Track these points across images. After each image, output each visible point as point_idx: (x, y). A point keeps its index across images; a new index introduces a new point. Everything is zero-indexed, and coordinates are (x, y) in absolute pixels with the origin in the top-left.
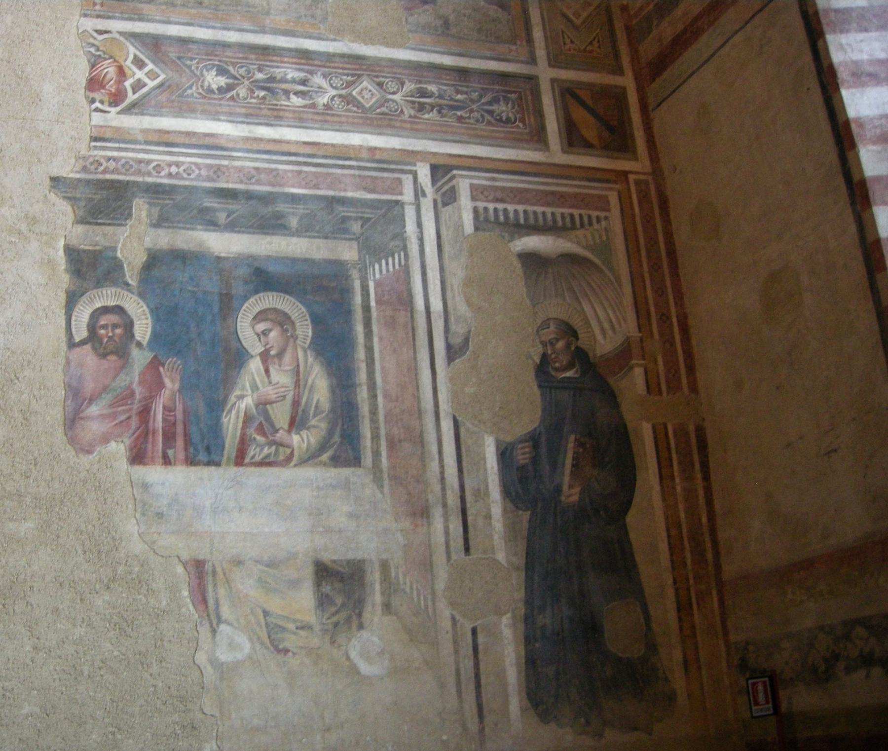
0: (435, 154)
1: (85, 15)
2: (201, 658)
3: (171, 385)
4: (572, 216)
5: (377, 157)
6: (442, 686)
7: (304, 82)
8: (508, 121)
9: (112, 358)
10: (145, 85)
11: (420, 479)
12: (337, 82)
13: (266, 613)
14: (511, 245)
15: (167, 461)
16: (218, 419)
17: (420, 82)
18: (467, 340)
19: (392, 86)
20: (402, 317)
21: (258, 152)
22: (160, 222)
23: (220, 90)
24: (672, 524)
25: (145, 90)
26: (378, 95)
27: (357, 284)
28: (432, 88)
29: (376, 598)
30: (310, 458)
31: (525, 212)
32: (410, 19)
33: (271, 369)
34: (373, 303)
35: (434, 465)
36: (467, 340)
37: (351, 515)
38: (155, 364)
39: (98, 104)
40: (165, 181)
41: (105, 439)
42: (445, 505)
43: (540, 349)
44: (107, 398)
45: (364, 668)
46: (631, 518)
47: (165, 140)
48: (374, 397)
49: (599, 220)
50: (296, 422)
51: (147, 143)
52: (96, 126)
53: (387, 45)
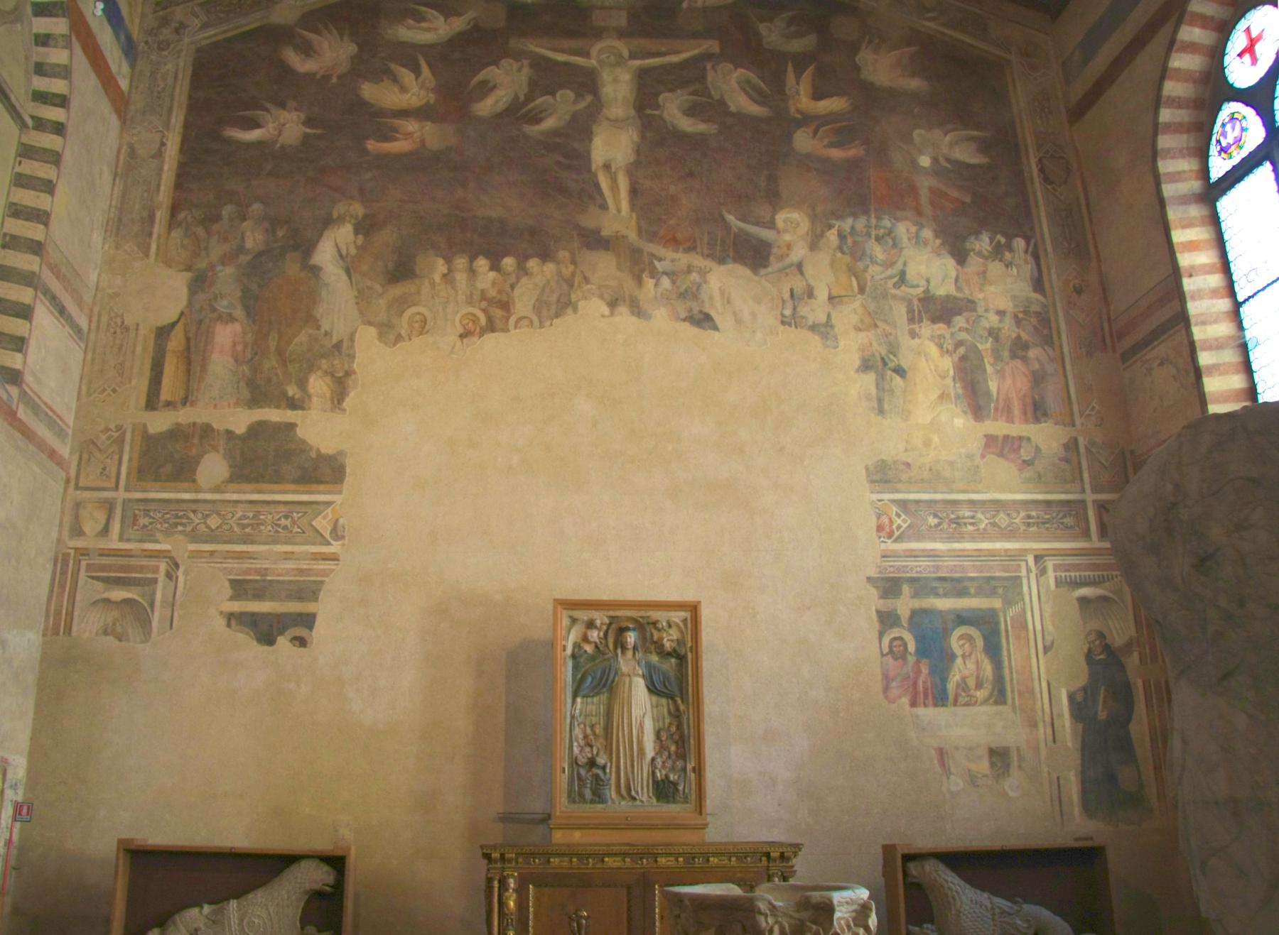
0: (1036, 550)
1: (872, 492)
2: (944, 789)
3: (925, 671)
4: (1103, 576)
5: (1009, 554)
7: (973, 517)
8: (1071, 527)
9: (900, 660)
10: (901, 527)
12: (988, 516)
13: (969, 770)
14: (1073, 594)
15: (925, 705)
16: (945, 685)
17: (1027, 511)
18: (1053, 643)
19: (1014, 515)
21: (954, 556)
22: (915, 595)
25: (902, 529)
26: (1008, 521)
28: (1034, 514)
29: (1015, 763)
30: (985, 702)
31: (1080, 576)
32: (1023, 476)
33: (967, 662)
34: (1009, 628)
35: (1039, 703)
36: (1053, 643)
38: (917, 662)
39: (882, 539)
40: (915, 575)
41: (900, 697)
42: (1044, 721)
43: (1088, 645)
45: (1011, 794)
47: (913, 554)
48: (1011, 673)
49: (1117, 576)
50: (979, 686)
51: (907, 557)
52: (883, 550)
53: (1010, 492)
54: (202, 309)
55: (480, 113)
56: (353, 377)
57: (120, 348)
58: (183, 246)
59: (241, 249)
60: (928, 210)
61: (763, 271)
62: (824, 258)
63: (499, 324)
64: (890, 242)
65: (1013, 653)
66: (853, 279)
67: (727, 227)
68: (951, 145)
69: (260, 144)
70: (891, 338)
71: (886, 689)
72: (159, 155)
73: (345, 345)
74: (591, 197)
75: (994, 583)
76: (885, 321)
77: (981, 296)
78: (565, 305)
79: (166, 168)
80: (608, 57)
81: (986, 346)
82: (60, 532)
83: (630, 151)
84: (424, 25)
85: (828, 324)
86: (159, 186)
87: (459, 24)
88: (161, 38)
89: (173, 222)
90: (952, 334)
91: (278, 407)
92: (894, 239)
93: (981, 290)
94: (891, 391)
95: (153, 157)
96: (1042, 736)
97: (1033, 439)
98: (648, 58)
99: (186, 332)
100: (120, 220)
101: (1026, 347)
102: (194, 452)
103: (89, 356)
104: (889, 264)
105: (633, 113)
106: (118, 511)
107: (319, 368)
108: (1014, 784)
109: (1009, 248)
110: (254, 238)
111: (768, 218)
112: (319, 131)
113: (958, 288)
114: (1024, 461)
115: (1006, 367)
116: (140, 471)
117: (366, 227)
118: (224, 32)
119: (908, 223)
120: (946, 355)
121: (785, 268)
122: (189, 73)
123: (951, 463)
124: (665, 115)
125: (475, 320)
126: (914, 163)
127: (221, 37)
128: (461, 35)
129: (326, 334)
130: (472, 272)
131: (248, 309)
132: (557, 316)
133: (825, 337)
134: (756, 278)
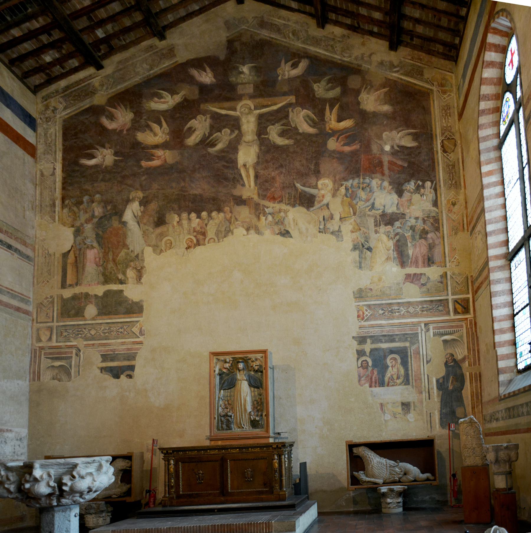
6: (424, 423)
7: (398, 309)
11: (421, 387)
12: (405, 308)
15: (375, 387)
19: (417, 307)
20: (418, 356)
23: (382, 314)
24: (472, 392)
27: (409, 351)
28: (425, 306)
29: (412, 408)
30: (400, 384)
35: (423, 384)
37: (408, 394)
38: (373, 370)
41: (365, 384)
44: (365, 377)
45: (410, 420)
46: (463, 392)
47: (372, 326)
50: (398, 378)
54: (80, 244)
55: (189, 144)
56: (144, 269)
57: (48, 263)
58: (69, 216)
59: (93, 216)
60: (386, 171)
61: (312, 209)
62: (338, 199)
63: (201, 242)
64: (369, 190)
65: (413, 364)
66: (351, 209)
67: (296, 189)
68: (400, 138)
69: (96, 166)
70: (367, 234)
71: (359, 381)
72: (53, 174)
73: (140, 256)
74: (238, 181)
75: (406, 336)
76: (364, 227)
77: (408, 211)
78: (228, 232)
79: (57, 180)
80: (244, 110)
81: (408, 234)
82: (32, 341)
83: (255, 157)
84: (162, 100)
85: (339, 231)
86: (55, 189)
87: (178, 98)
88: (47, 115)
89: (63, 206)
90: (394, 230)
91: (115, 284)
92: (370, 188)
93: (408, 208)
94: (365, 258)
95: (51, 175)
96: (424, 397)
97: (427, 274)
98: (263, 109)
99: (75, 254)
100: (41, 206)
101: (427, 233)
102: (83, 304)
103: (36, 268)
104: (367, 200)
105: (256, 138)
106: (55, 331)
107: (131, 266)
108: (411, 417)
109: (423, 187)
110: (98, 211)
111: (314, 184)
112: (121, 158)
113: (398, 209)
114: (422, 284)
115: (417, 243)
116: (62, 314)
117: (144, 203)
118: (74, 111)
119: (377, 180)
120: (391, 240)
121: (321, 207)
122: (61, 132)
123: (390, 287)
124: (270, 138)
125: (192, 241)
126: (382, 150)
127: (73, 113)
128: (178, 104)
129: (132, 251)
130: (189, 219)
131: (98, 242)
132: (225, 237)
133: (337, 236)
134: (309, 212)
